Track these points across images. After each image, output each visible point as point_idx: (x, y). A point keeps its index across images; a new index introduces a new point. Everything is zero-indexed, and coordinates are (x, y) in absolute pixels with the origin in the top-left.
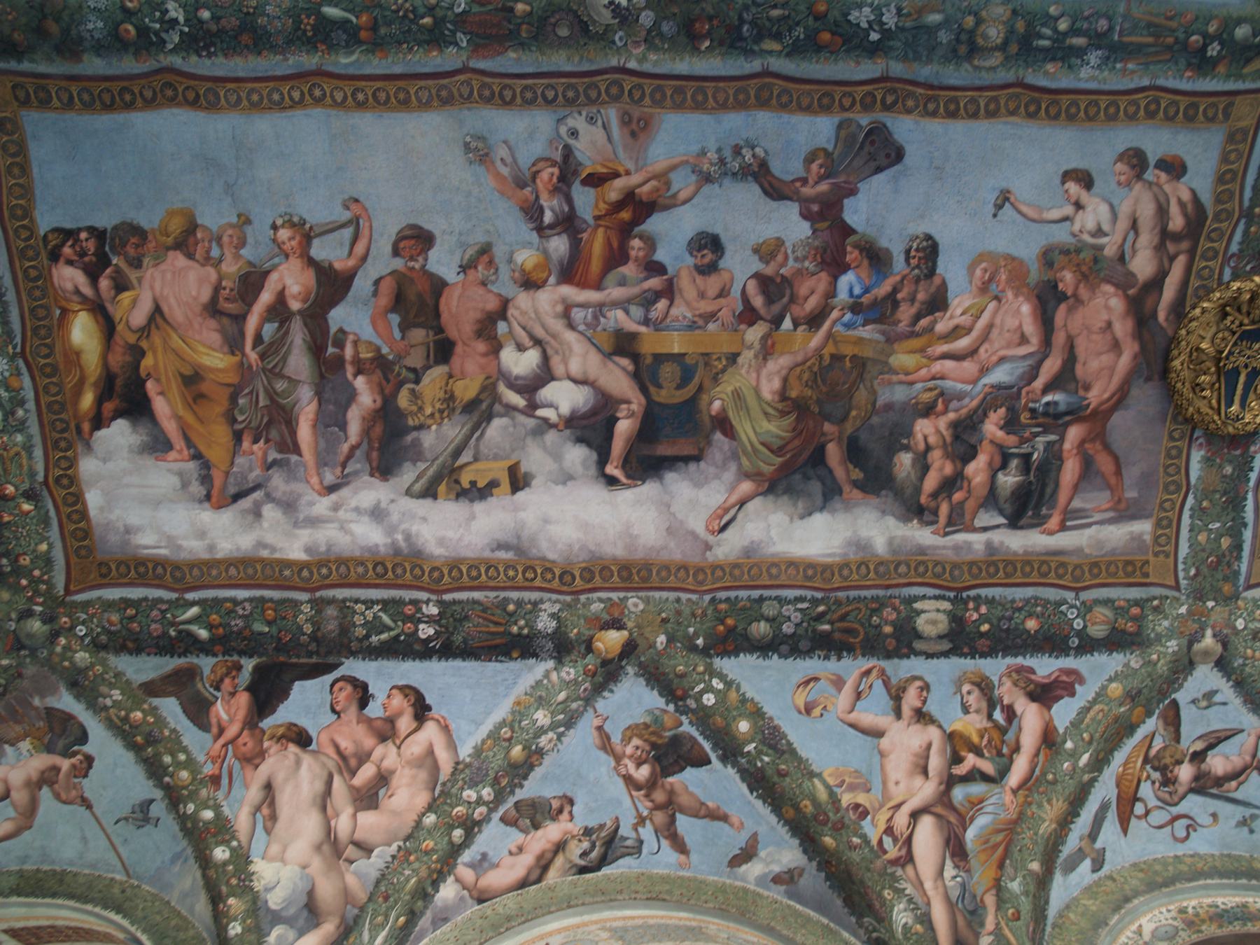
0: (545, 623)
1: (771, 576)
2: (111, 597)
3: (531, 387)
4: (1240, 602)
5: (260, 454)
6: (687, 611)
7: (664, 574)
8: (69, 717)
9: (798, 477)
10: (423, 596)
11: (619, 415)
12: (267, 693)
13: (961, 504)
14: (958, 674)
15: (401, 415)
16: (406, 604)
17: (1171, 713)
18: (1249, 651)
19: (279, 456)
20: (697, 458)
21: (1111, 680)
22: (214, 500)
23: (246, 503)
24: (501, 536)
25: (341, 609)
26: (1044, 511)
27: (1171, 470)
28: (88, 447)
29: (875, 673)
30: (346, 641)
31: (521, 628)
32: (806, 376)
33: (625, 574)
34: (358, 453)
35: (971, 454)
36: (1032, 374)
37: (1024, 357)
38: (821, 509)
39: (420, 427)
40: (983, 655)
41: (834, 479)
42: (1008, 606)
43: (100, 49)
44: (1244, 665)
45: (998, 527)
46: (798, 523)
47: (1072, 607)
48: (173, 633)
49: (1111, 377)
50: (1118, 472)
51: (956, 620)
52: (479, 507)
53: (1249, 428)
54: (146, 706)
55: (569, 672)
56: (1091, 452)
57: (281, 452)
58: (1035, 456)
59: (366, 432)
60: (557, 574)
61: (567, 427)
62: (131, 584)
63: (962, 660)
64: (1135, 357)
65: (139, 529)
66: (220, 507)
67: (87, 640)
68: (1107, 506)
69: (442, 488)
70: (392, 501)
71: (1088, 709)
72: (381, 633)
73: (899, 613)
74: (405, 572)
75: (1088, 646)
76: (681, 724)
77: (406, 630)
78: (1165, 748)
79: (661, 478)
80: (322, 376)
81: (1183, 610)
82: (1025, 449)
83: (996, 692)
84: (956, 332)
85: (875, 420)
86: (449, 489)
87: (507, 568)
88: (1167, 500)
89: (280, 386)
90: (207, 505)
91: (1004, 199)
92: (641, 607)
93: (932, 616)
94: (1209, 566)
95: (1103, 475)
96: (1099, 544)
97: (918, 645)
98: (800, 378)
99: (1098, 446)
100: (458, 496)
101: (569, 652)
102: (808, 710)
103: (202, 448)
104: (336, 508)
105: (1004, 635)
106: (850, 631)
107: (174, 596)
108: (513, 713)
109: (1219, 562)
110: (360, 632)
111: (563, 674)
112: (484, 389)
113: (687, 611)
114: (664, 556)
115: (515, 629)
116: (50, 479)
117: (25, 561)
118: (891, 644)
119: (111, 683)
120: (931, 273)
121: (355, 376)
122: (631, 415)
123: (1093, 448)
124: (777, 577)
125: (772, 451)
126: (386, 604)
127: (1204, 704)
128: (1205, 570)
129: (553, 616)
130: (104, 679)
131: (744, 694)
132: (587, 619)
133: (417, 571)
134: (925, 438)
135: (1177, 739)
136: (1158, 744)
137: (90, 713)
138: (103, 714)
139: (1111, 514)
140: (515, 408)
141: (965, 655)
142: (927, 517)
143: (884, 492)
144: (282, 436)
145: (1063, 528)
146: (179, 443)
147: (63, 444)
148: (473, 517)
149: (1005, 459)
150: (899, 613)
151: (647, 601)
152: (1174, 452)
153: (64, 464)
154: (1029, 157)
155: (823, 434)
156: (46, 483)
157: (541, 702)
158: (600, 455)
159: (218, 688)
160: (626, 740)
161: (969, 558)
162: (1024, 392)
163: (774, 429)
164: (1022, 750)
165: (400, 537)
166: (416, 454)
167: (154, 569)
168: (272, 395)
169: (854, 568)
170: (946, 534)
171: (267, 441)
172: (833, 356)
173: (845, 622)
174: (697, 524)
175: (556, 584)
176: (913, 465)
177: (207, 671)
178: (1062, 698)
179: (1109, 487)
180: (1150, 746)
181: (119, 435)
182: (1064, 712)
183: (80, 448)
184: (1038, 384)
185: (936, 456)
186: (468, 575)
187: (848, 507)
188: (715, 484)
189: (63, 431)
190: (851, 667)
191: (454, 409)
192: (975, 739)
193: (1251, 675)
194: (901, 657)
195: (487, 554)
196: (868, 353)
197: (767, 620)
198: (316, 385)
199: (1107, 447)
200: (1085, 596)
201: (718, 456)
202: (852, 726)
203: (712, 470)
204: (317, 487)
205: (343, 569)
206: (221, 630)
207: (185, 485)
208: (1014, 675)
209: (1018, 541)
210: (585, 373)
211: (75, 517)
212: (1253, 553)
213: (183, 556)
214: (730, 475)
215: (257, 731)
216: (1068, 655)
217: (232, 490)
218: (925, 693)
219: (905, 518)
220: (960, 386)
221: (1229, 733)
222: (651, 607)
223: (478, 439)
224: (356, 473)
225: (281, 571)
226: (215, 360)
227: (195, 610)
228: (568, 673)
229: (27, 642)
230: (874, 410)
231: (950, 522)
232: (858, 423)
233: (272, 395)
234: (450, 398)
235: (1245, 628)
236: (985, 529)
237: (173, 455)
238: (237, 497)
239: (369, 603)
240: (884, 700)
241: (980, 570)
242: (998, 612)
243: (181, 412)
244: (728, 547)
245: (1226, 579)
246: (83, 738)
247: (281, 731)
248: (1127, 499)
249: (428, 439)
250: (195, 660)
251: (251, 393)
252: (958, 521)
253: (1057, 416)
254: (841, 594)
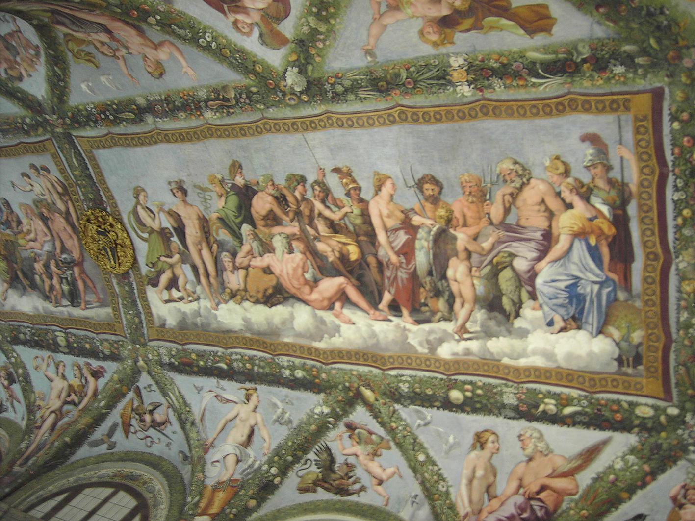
21: (115, 373)
50: (95, 287)
51: (67, 341)
75: (105, 358)
84: (29, 232)
91: (13, 185)
106: (42, 341)
120: (12, 212)
123: (83, 276)
127: (148, 389)
139: (97, 304)
149: (61, 278)
170: (57, 307)
182: (102, 382)
185: (44, 276)
190: (45, 354)
192: (76, 388)
219: (45, 301)
236: (66, 306)
254: (37, 326)
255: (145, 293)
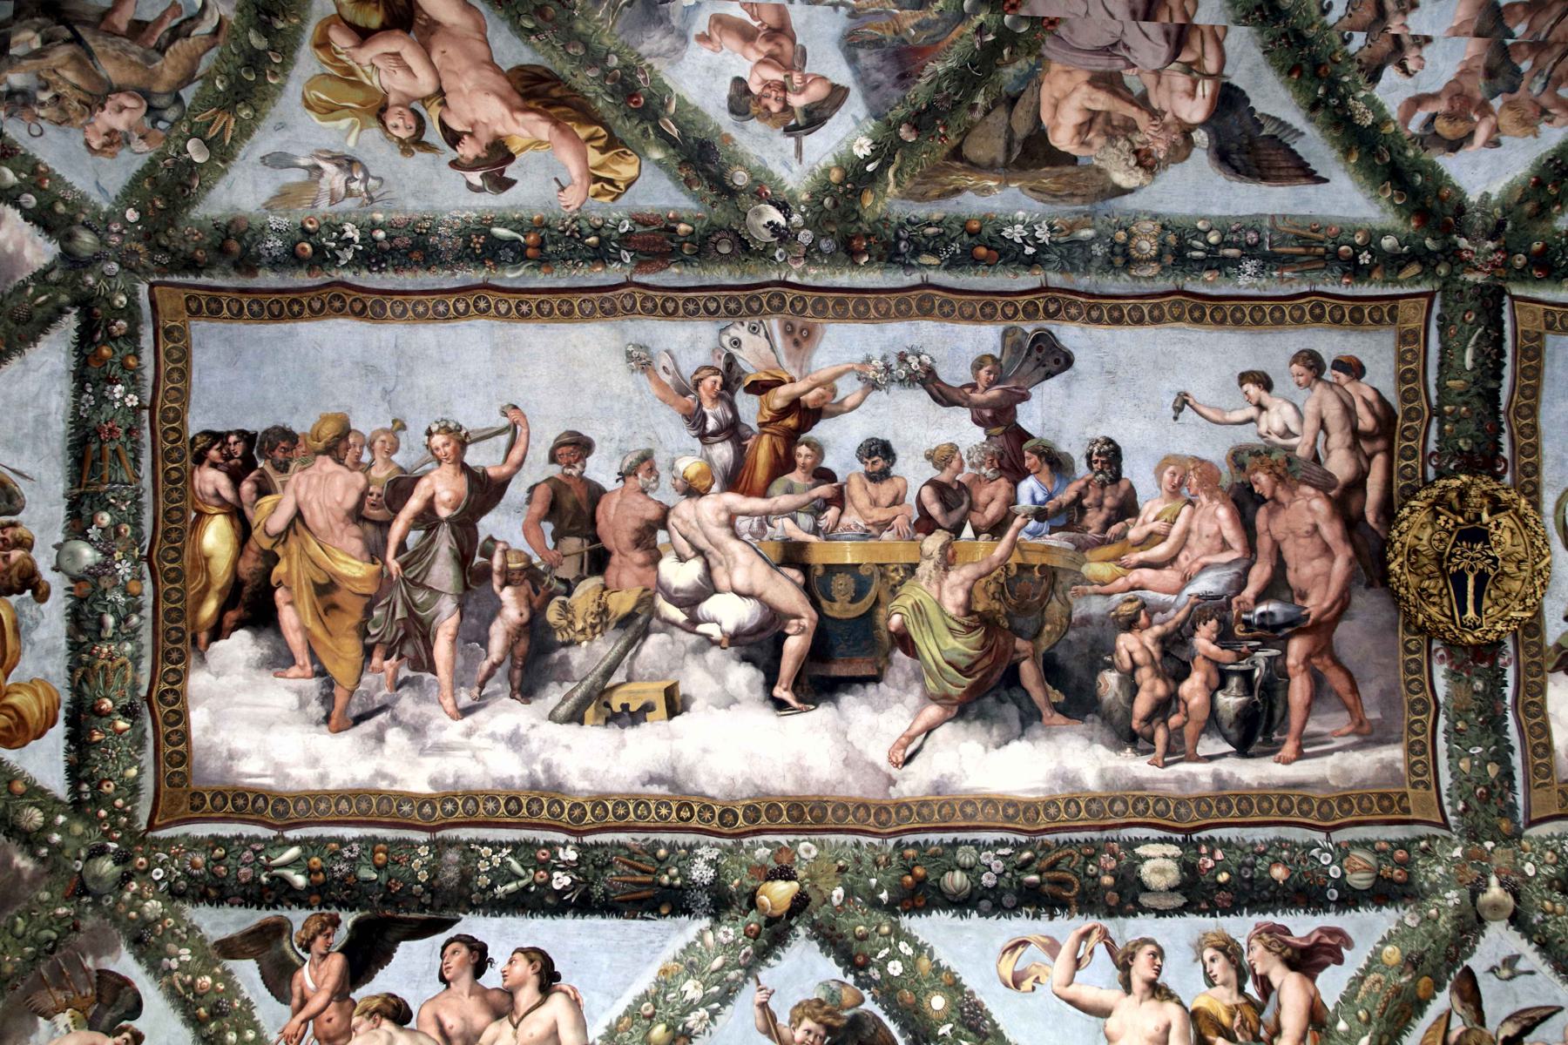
0: (701, 872)
1: (965, 816)
2: (199, 834)
3: (691, 601)
4: (1524, 843)
5: (391, 671)
6: (868, 858)
7: (840, 813)
8: (125, 983)
9: (990, 700)
10: (561, 837)
11: (788, 631)
12: (365, 956)
13: (1180, 729)
14: (1197, 935)
15: (549, 629)
16: (539, 847)
17: (1467, 986)
18: (1547, 903)
19: (411, 674)
20: (876, 679)
21: (1384, 942)
22: (333, 722)
23: (368, 726)
24: (655, 768)
25: (464, 853)
26: (1276, 736)
27: (1414, 686)
28: (202, 659)
29: (1095, 935)
30: (466, 891)
31: (672, 878)
32: (992, 588)
33: (795, 813)
34: (499, 671)
35: (1181, 672)
36: (1241, 582)
37: (1229, 564)
38: (1020, 737)
39: (569, 644)
40: (1226, 912)
41: (1031, 701)
42: (1248, 850)
43: (276, 264)
44: (1546, 921)
45: (1224, 755)
46: (994, 753)
47: (1324, 850)
48: (264, 879)
49: (1328, 583)
50: (1354, 690)
51: (1188, 868)
52: (631, 733)
53: (1490, 636)
54: (218, 970)
55: (728, 932)
56: (1319, 668)
57: (413, 669)
58: (1257, 673)
59: (510, 648)
60: (717, 812)
61: (730, 645)
62: (225, 819)
63: (1200, 918)
64: (1350, 561)
65: (245, 754)
66: (339, 731)
67: (163, 886)
68: (1346, 730)
69: (590, 713)
70: (533, 726)
71: (1362, 980)
72: (509, 882)
73: (1119, 860)
74: (541, 809)
75: (1350, 899)
76: (863, 1000)
77: (538, 879)
78: (1467, 1032)
79: (836, 702)
80: (466, 587)
81: (1458, 852)
82: (1244, 665)
83: (1246, 959)
85: (1072, 635)
86: (598, 713)
87: (659, 804)
88: (1416, 721)
89: (420, 597)
90: (324, 728)
92: (814, 852)
93: (1159, 865)
94: (1479, 799)
95: (1338, 694)
96: (1346, 773)
97: (1145, 900)
98: (985, 590)
99: (1328, 662)
100: (607, 721)
101: (728, 907)
102: (1017, 982)
103: (327, 664)
104: (469, 733)
105: (1247, 886)
106: (1062, 883)
107: (273, 833)
108: (658, 983)
109: (1489, 794)
110: (484, 881)
111: (720, 935)
112: (640, 602)
113: (868, 858)
114: (842, 792)
115: (665, 879)
116: (154, 694)
117: (109, 788)
118: (1112, 898)
119: (181, 940)
121: (502, 587)
122: (802, 631)
124: (972, 817)
125: (959, 671)
126: (516, 847)
127: (1506, 973)
128: (1475, 803)
129: (710, 863)
130: (174, 935)
131: (937, 962)
132: (750, 868)
133: (556, 808)
134: (1131, 654)
135: (1481, 1020)
136: (1457, 1027)
137: (150, 977)
138: (165, 979)
140: (674, 624)
141: (1202, 912)
142: (1142, 744)
143: (1089, 717)
144: (417, 653)
145: (1301, 756)
146: (302, 657)
147: (175, 656)
148: (623, 744)
150: (1119, 860)
151: (821, 846)
152: (1413, 666)
153: (172, 678)
154: (1206, 359)
155: (1016, 651)
156: (148, 698)
157: (692, 969)
158: (767, 675)
159: (307, 949)
160: (796, 1021)
161: (1196, 792)
162: (1234, 602)
163: (962, 646)
164: (1285, 1033)
165: (538, 768)
166: (563, 673)
167: (254, 802)
168: (410, 606)
169: (1062, 806)
170: (1166, 765)
171: (400, 657)
172: (1019, 566)
173: (1056, 873)
174: (878, 754)
175: (715, 825)
176: (1120, 687)
177: (297, 927)
178: (1326, 965)
179: (1349, 710)
180: (1447, 1030)
181: (240, 646)
182: (1332, 983)
183: (193, 660)
184: (1249, 592)
185: (1144, 675)
186: (614, 814)
187: (1049, 736)
188: (897, 709)
189: (178, 641)
190: (1067, 927)
191: (607, 624)
192: (1225, 1019)
193: (1556, 935)
194: (1126, 915)
195: (638, 788)
196: (1057, 562)
197: (963, 869)
198: (460, 596)
199: (1337, 662)
200: (1338, 836)
201: (900, 677)
202: (1071, 1002)
203: (893, 692)
204: (450, 709)
205: (471, 804)
206: (321, 876)
207: (303, 705)
208: (1265, 936)
209: (1252, 772)
210: (751, 585)
211: (174, 738)
212: (1527, 782)
213: (291, 786)
214: (914, 698)
215: (347, 1003)
216: (1327, 911)
217: (355, 711)
218: (1158, 961)
219: (1117, 747)
220: (1162, 597)
221: (1545, 1012)
222: (826, 854)
223: (632, 658)
224: (495, 694)
225: (399, 805)
226: (353, 568)
227: (294, 852)
228: (726, 933)
229: (92, 886)
230: (1070, 625)
231: (1169, 751)
232: (1054, 639)
233: (410, 606)
234: (604, 611)
235: (1537, 874)
236: (1210, 758)
237: (294, 671)
238: (358, 720)
239: (497, 846)
240: (1113, 972)
241: (1210, 806)
242: (1237, 857)
243: (310, 623)
244: (914, 782)
245: (1501, 814)
246: (136, 1009)
247: (376, 1003)
248: (1370, 721)
249: (577, 656)
250: (286, 913)
251: (388, 604)
252: (1177, 750)
253: (1276, 628)
255: (1542, 690)
